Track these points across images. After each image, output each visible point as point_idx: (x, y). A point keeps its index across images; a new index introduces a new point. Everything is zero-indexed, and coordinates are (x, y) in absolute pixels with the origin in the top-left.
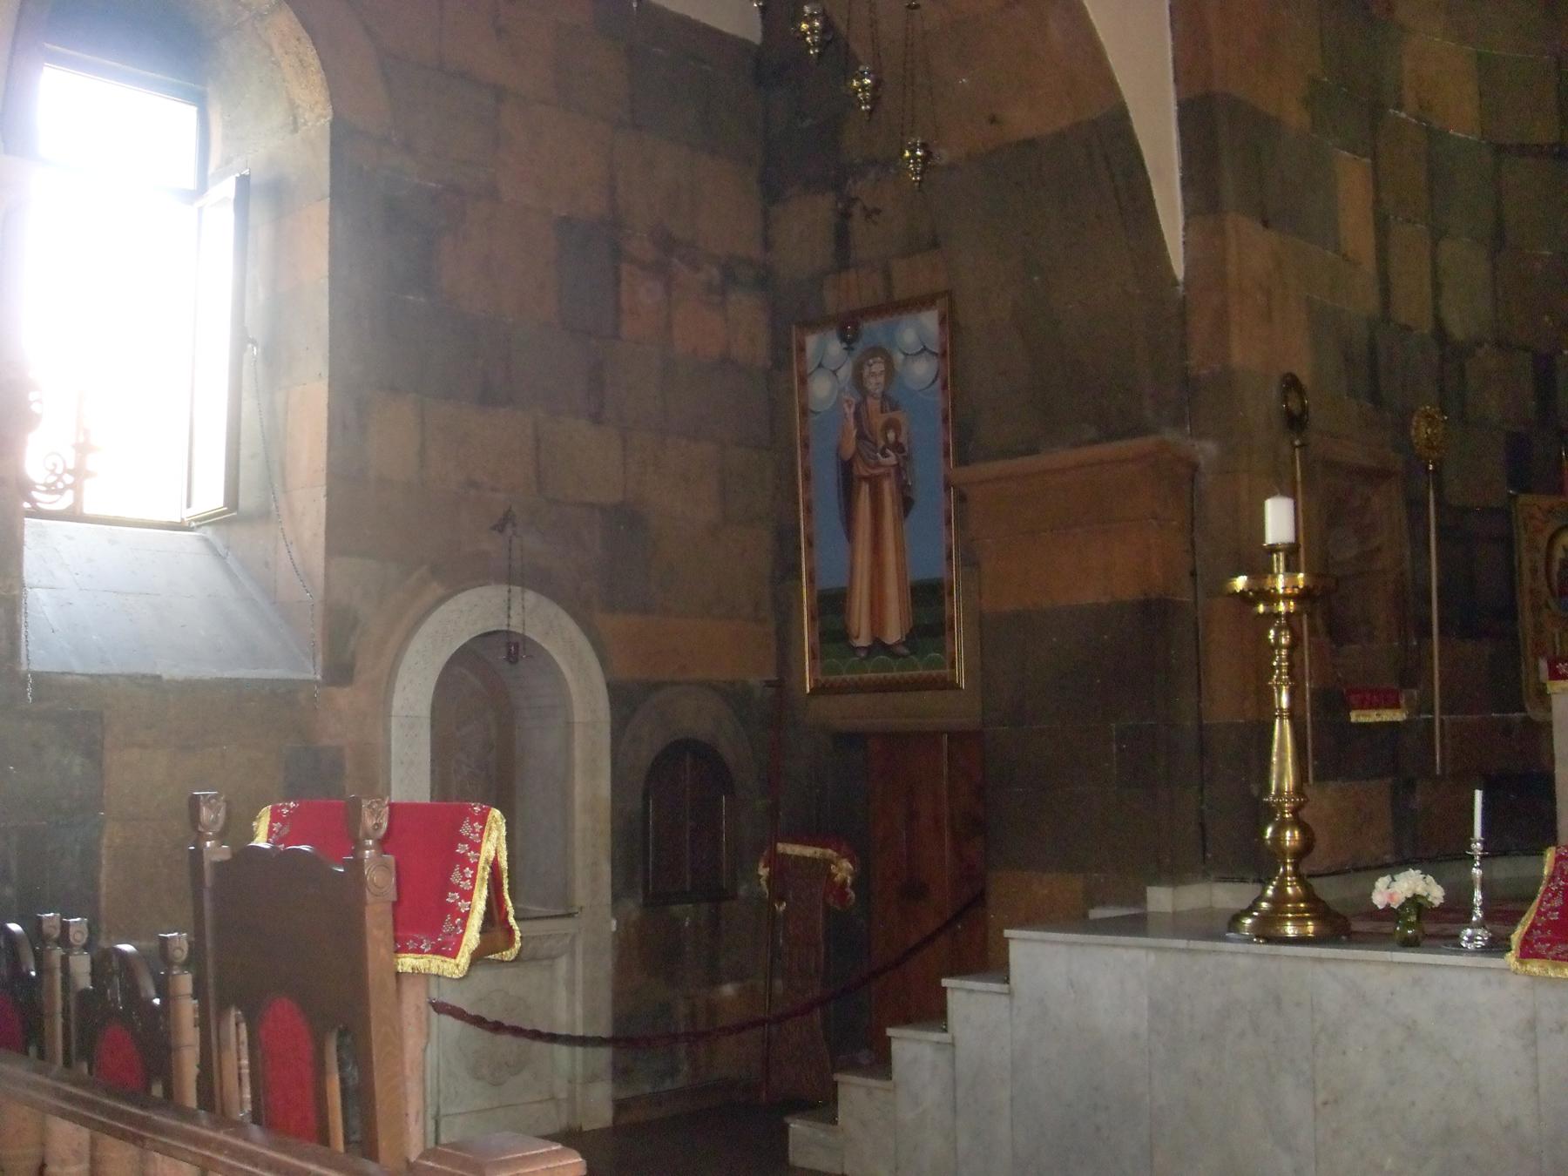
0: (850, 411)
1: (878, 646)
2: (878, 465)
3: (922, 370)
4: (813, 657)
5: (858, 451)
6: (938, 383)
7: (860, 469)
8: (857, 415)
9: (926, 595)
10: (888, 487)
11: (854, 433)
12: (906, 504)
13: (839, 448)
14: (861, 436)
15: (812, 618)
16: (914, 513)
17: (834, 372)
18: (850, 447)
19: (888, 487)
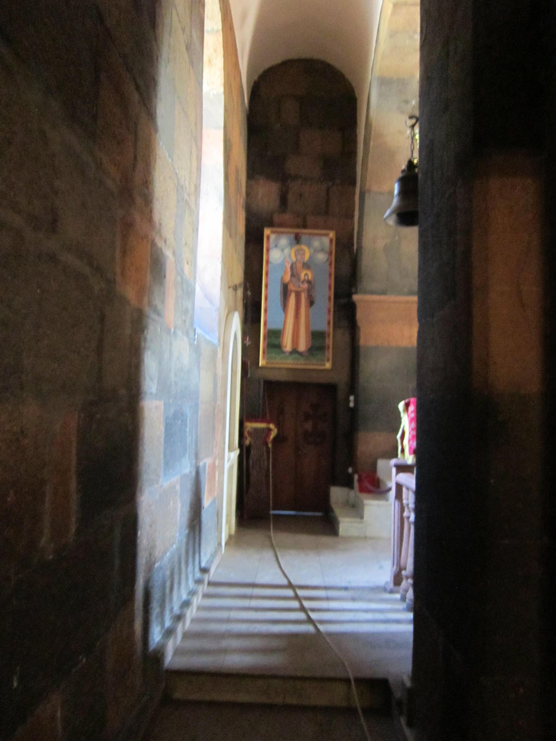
0: (288, 266)
1: (295, 351)
2: (299, 287)
3: (322, 257)
4: (264, 353)
5: (291, 280)
6: (328, 263)
7: (291, 287)
8: (292, 268)
9: (317, 337)
10: (303, 296)
11: (290, 274)
12: (311, 303)
13: (282, 279)
14: (292, 275)
15: (264, 339)
16: (313, 307)
17: (283, 250)
18: (288, 278)
19: (303, 296)
